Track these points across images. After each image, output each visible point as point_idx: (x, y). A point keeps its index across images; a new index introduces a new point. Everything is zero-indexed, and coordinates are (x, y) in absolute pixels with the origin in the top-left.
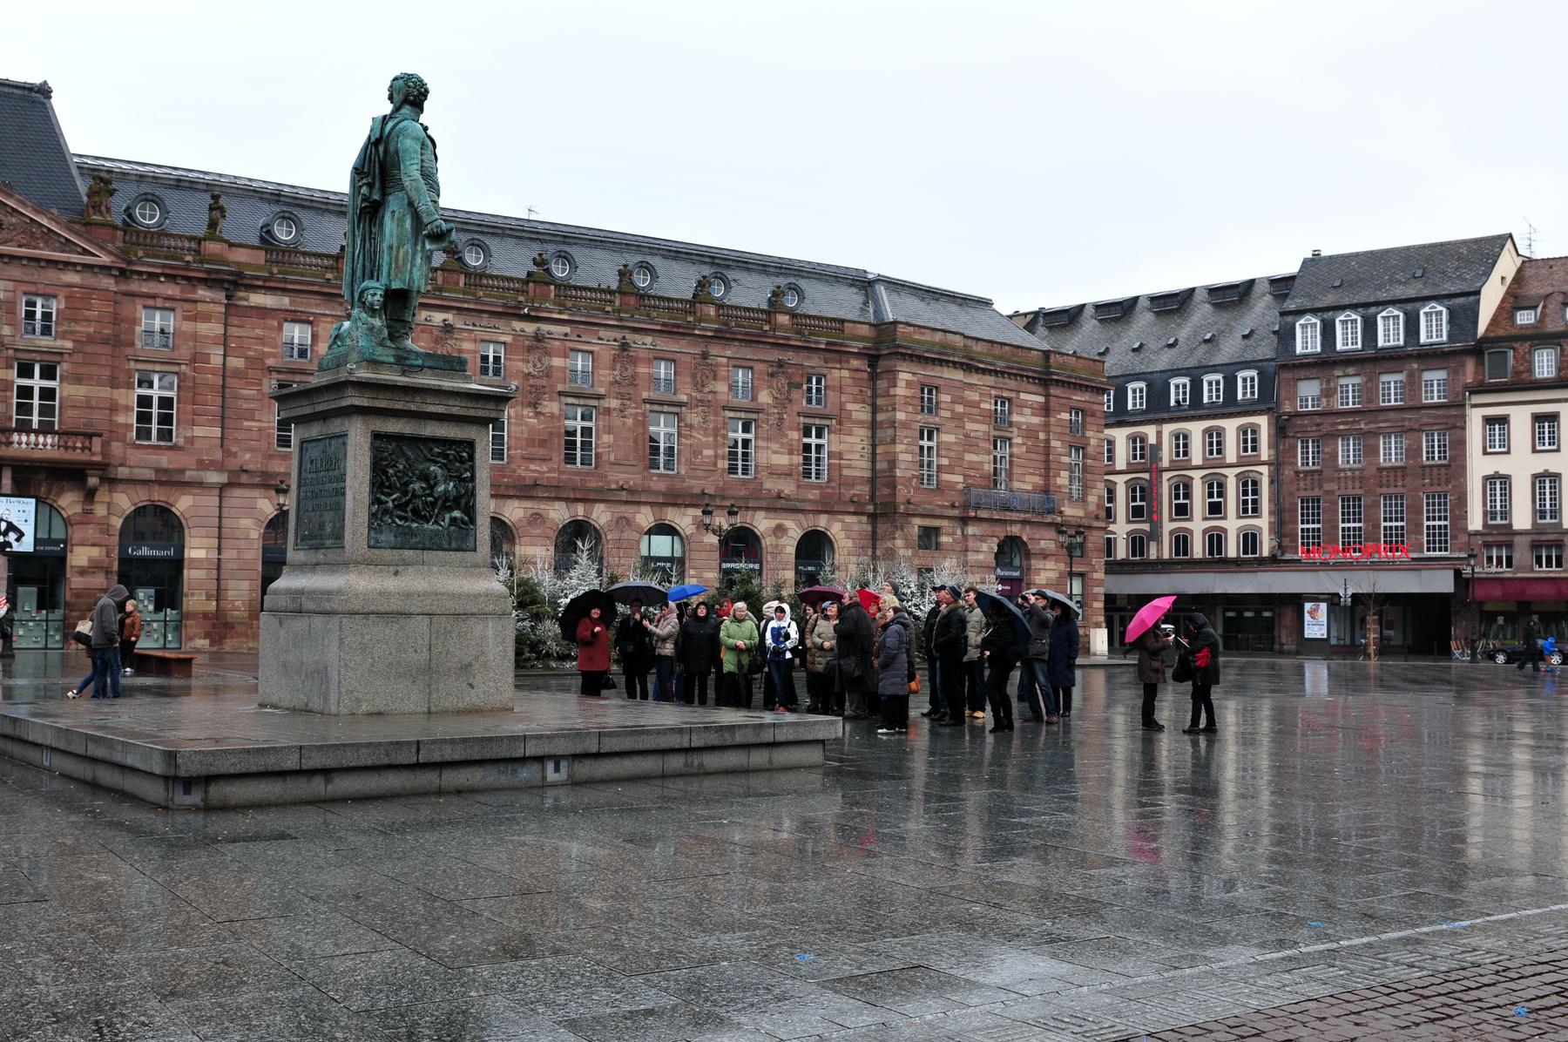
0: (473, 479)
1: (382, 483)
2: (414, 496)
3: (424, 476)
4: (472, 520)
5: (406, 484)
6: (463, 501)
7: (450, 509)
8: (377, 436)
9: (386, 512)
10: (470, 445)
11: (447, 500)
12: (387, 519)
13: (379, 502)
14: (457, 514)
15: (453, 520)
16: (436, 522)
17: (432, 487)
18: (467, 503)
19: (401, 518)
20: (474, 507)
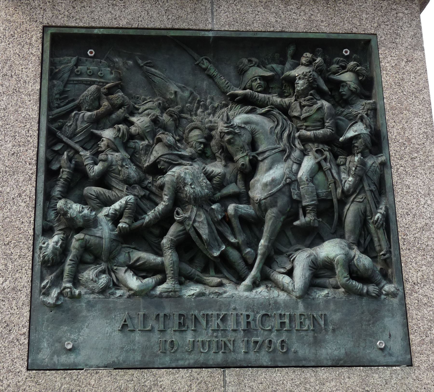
6: (351, 212)
7: (312, 236)
9: (90, 255)
11: (294, 208)
16: (264, 279)
18: (363, 220)
19: (140, 270)
20: (388, 224)
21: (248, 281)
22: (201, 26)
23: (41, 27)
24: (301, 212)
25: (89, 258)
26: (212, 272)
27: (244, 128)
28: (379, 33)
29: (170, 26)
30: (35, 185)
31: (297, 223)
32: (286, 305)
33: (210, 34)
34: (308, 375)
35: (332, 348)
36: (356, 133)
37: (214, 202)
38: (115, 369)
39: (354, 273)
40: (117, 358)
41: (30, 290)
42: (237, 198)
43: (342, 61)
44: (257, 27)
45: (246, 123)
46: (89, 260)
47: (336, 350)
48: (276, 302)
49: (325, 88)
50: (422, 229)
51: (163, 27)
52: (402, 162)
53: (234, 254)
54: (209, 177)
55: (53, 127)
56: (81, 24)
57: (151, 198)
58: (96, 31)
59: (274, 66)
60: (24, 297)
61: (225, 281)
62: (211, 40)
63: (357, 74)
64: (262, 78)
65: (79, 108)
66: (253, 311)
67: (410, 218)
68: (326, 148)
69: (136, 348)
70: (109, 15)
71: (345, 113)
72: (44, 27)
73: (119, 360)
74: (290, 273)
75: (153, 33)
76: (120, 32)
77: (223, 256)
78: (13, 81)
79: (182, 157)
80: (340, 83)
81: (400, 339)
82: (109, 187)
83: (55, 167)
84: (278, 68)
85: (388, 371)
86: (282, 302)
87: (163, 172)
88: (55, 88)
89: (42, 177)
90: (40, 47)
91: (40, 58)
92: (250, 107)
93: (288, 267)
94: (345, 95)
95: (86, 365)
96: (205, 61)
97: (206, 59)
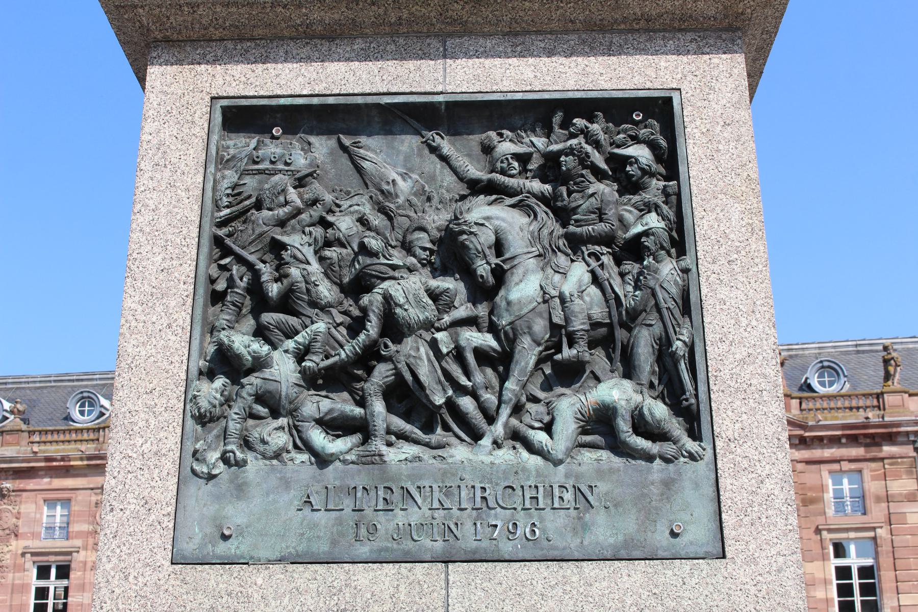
0: (679, 241)
1: (256, 289)
2: (394, 328)
3: (451, 253)
4: (693, 420)
5: (358, 286)
8: (240, 117)
10: (660, 110)
12: (274, 433)
13: (225, 364)
14: (616, 392)
15: (600, 425)
17: (485, 291)
19: (336, 426)
21: (486, 442)
22: (428, 89)
23: (208, 99)
24: (565, 340)
25: (261, 410)
26: (439, 430)
27: (482, 225)
28: (684, 87)
29: (385, 90)
30: (190, 312)
31: (558, 357)
32: (539, 474)
33: (440, 98)
34: (569, 571)
35: (603, 531)
36: (646, 228)
37: (439, 330)
38: (292, 563)
39: (642, 425)
40: (294, 548)
41: (178, 454)
42: (471, 322)
43: (632, 129)
44: (506, 85)
45: (488, 218)
46: (263, 415)
47: (610, 536)
48: (524, 469)
49: (603, 166)
50: (743, 361)
51: (374, 91)
52: (716, 268)
53: (467, 403)
54: (434, 296)
55: (221, 232)
56: (262, 93)
57: (356, 326)
58: (282, 101)
59: (535, 139)
60: (169, 465)
61: (453, 440)
62: (443, 107)
63: (653, 146)
64: (517, 156)
65: (258, 205)
66: (491, 483)
67: (724, 347)
68: (605, 250)
69: (322, 534)
70: (300, 79)
71: (633, 201)
72: (212, 98)
73: (297, 551)
74: (548, 428)
75: (360, 100)
76: (315, 101)
77: (451, 405)
78: (167, 173)
79: (394, 267)
80: (626, 160)
81: (706, 520)
82: (296, 313)
83: (221, 286)
84: (540, 142)
85: (687, 565)
86: (533, 469)
87: (369, 289)
88: (225, 181)
89: (200, 301)
90: (206, 125)
91: (206, 141)
92: (494, 197)
93: (547, 419)
94: (633, 176)
95: (252, 558)
96: (436, 137)
97: (437, 134)
